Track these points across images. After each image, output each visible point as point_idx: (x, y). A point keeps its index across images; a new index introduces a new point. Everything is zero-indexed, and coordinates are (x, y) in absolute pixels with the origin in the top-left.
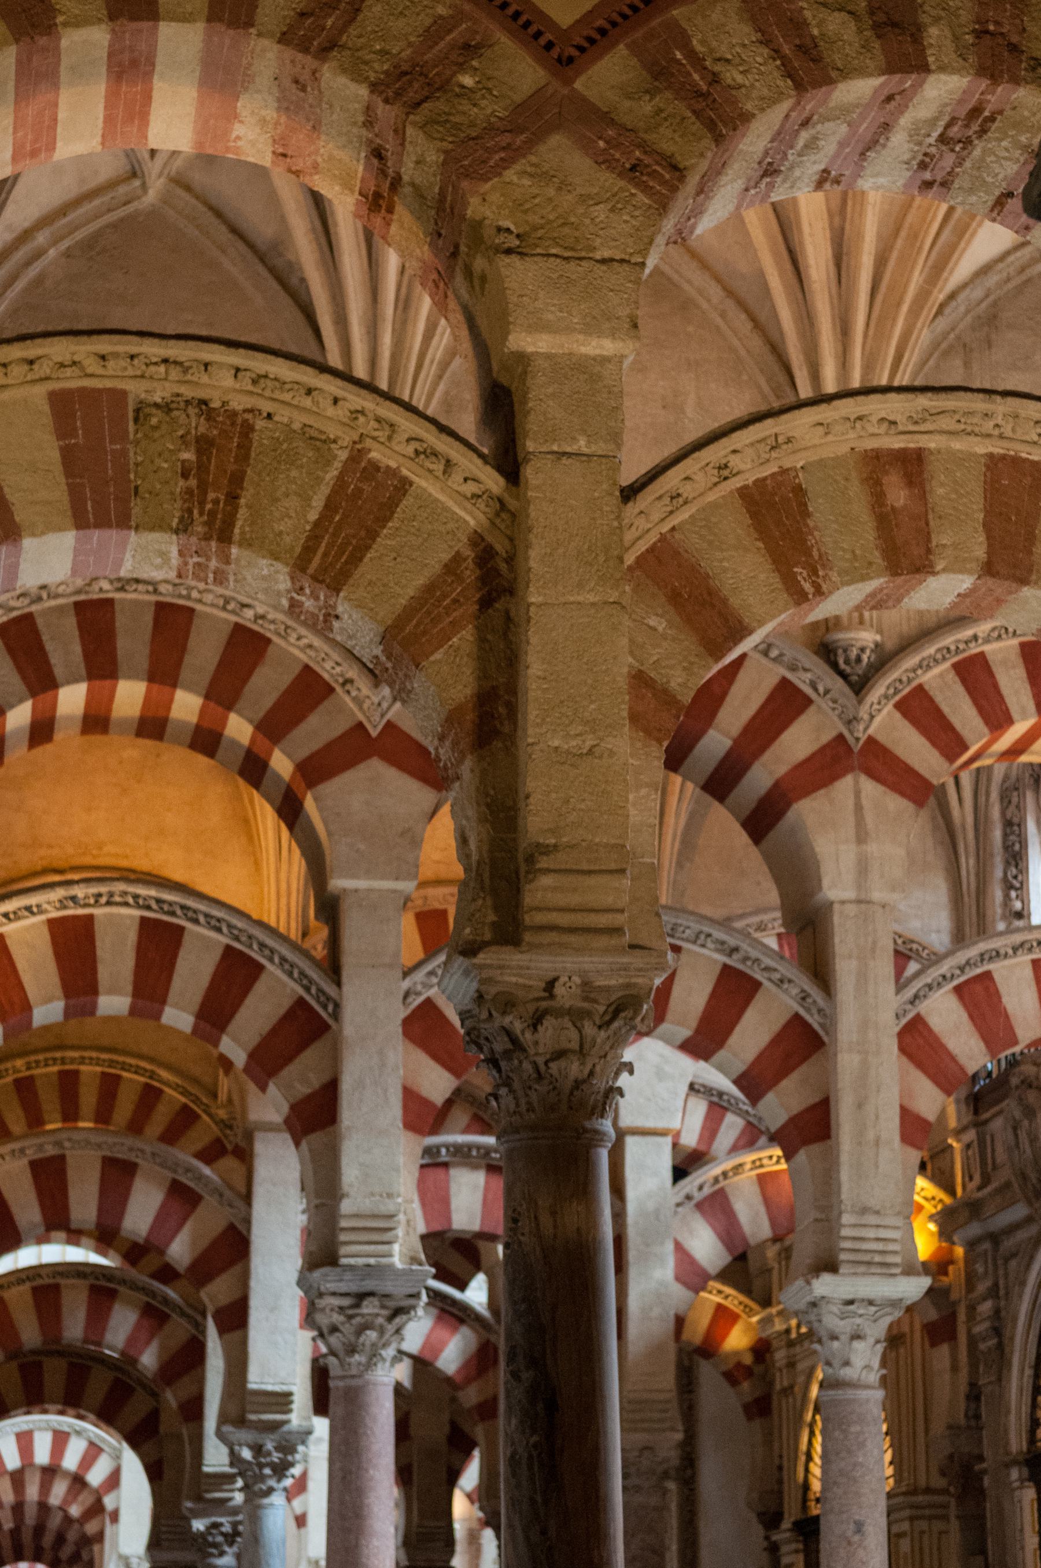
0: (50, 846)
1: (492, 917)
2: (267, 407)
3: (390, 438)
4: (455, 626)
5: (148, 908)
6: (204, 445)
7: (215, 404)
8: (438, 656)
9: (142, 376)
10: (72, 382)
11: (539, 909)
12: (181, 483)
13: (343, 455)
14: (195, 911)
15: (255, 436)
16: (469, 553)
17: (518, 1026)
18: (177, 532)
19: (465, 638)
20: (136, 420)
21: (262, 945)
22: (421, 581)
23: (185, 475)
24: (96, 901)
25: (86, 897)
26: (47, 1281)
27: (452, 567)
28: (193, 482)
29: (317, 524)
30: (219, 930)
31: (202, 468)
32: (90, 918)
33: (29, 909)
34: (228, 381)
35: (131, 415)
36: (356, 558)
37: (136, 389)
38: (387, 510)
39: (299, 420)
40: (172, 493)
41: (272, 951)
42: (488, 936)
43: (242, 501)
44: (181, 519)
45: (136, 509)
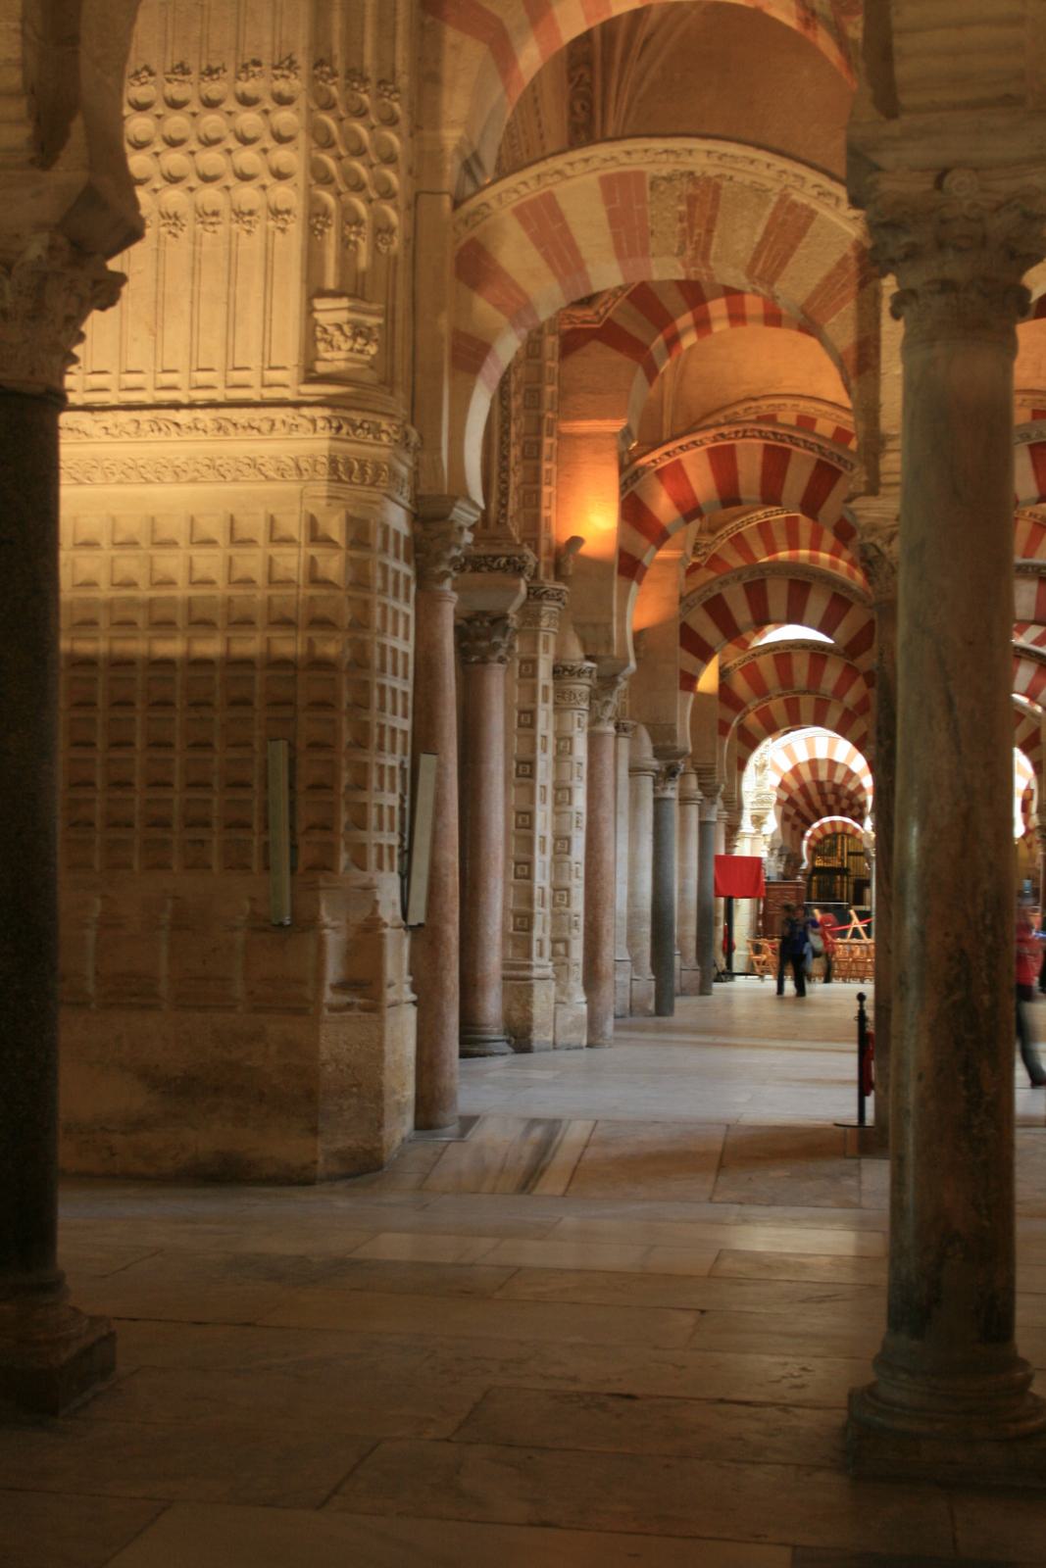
1: (864, 478)
2: (729, 173)
3: (802, 186)
4: (843, 301)
5: (768, 438)
6: (692, 201)
7: (698, 174)
8: (833, 320)
9: (653, 162)
10: (612, 169)
11: (889, 473)
12: (679, 225)
13: (775, 199)
14: (797, 439)
15: (722, 192)
16: (852, 254)
17: (879, 543)
18: (677, 255)
19: (849, 308)
20: (651, 188)
22: (822, 274)
23: (681, 220)
27: (842, 264)
28: (685, 224)
29: (760, 244)
30: (811, 449)
31: (691, 214)
32: (732, 447)
33: (694, 443)
34: (703, 159)
35: (648, 185)
36: (783, 264)
37: (651, 170)
38: (802, 231)
39: (748, 179)
40: (674, 232)
42: (862, 489)
43: (715, 234)
44: (679, 247)
45: (653, 245)
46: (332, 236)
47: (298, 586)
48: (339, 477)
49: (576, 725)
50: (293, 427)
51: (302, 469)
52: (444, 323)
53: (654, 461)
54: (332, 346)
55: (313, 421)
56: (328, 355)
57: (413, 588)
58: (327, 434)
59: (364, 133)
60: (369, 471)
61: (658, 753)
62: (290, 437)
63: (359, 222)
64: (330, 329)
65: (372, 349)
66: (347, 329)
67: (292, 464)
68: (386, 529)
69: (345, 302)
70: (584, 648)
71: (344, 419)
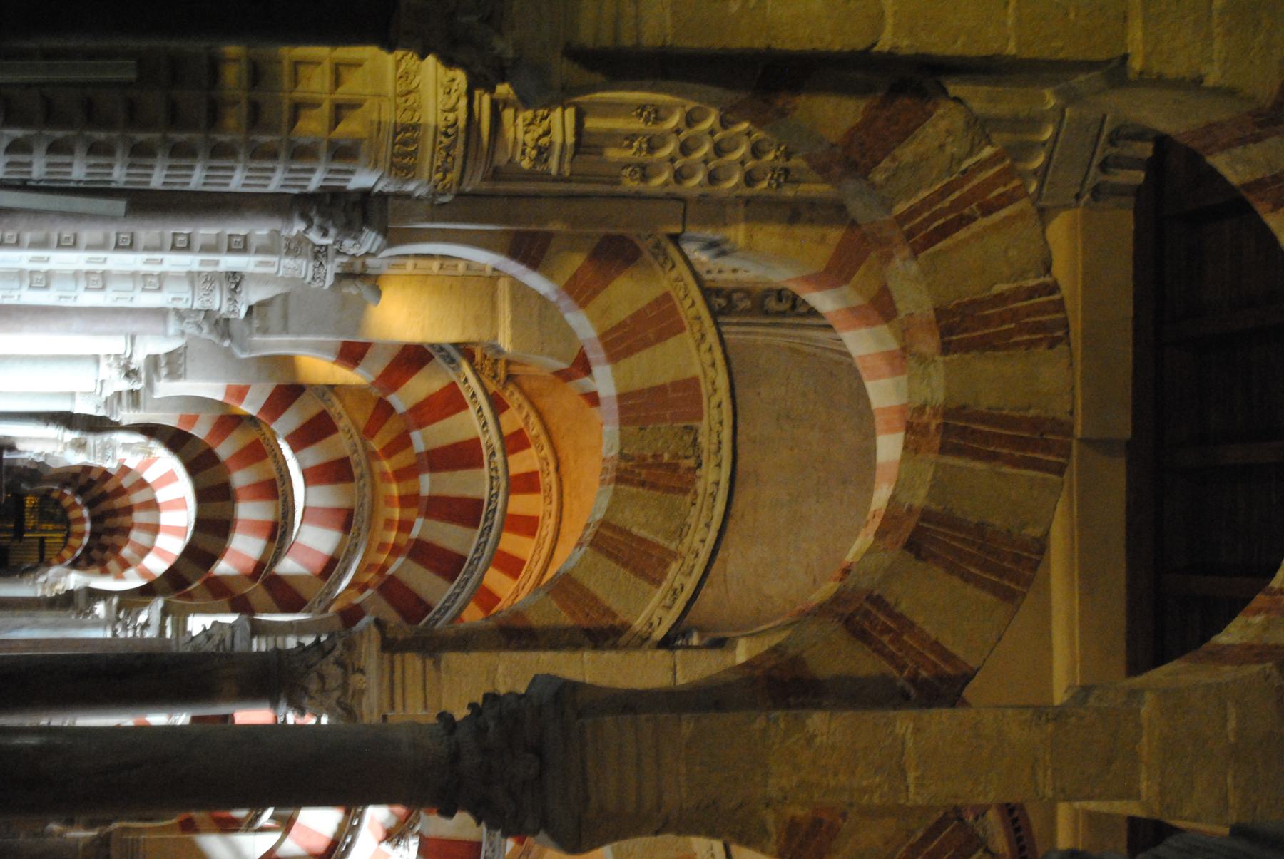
0: (576, 461)
1: (400, 637)
2: (699, 501)
3: (683, 574)
4: (573, 614)
5: (489, 504)
6: (673, 467)
7: (698, 472)
8: (555, 605)
9: (711, 430)
10: (705, 388)
11: (403, 661)
12: (650, 454)
13: (673, 547)
14: (488, 534)
15: (681, 496)
16: (617, 622)
17: (336, 653)
18: (621, 453)
19: (565, 620)
20: (686, 427)
21: (467, 580)
22: (600, 593)
23: (654, 456)
24: (492, 469)
25: (495, 462)
26: (280, 490)
27: (608, 612)
28: (650, 460)
29: (629, 534)
30: (477, 550)
31: (660, 465)
32: (481, 465)
33: (485, 424)
34: (712, 478)
35: (690, 424)
36: (610, 555)
37: (703, 426)
38: (639, 572)
39: (692, 520)
40: (643, 449)
41: (463, 588)
42: (389, 636)
43: (641, 490)
44: (628, 455)
45: (632, 429)
46: (637, 125)
47: (291, 92)
48: (399, 133)
49: (177, 296)
50: (448, 90)
51: (409, 96)
52: (556, 226)
53: (466, 380)
54: (529, 124)
55: (453, 109)
56: (520, 120)
57: (296, 191)
58: (442, 124)
59: (737, 155)
60: (406, 161)
61: (153, 361)
62: (439, 85)
63: (652, 149)
64: (545, 123)
65: (526, 164)
66: (544, 141)
67: (414, 85)
68: (352, 172)
69: (570, 140)
70: (262, 304)
71: (456, 140)
